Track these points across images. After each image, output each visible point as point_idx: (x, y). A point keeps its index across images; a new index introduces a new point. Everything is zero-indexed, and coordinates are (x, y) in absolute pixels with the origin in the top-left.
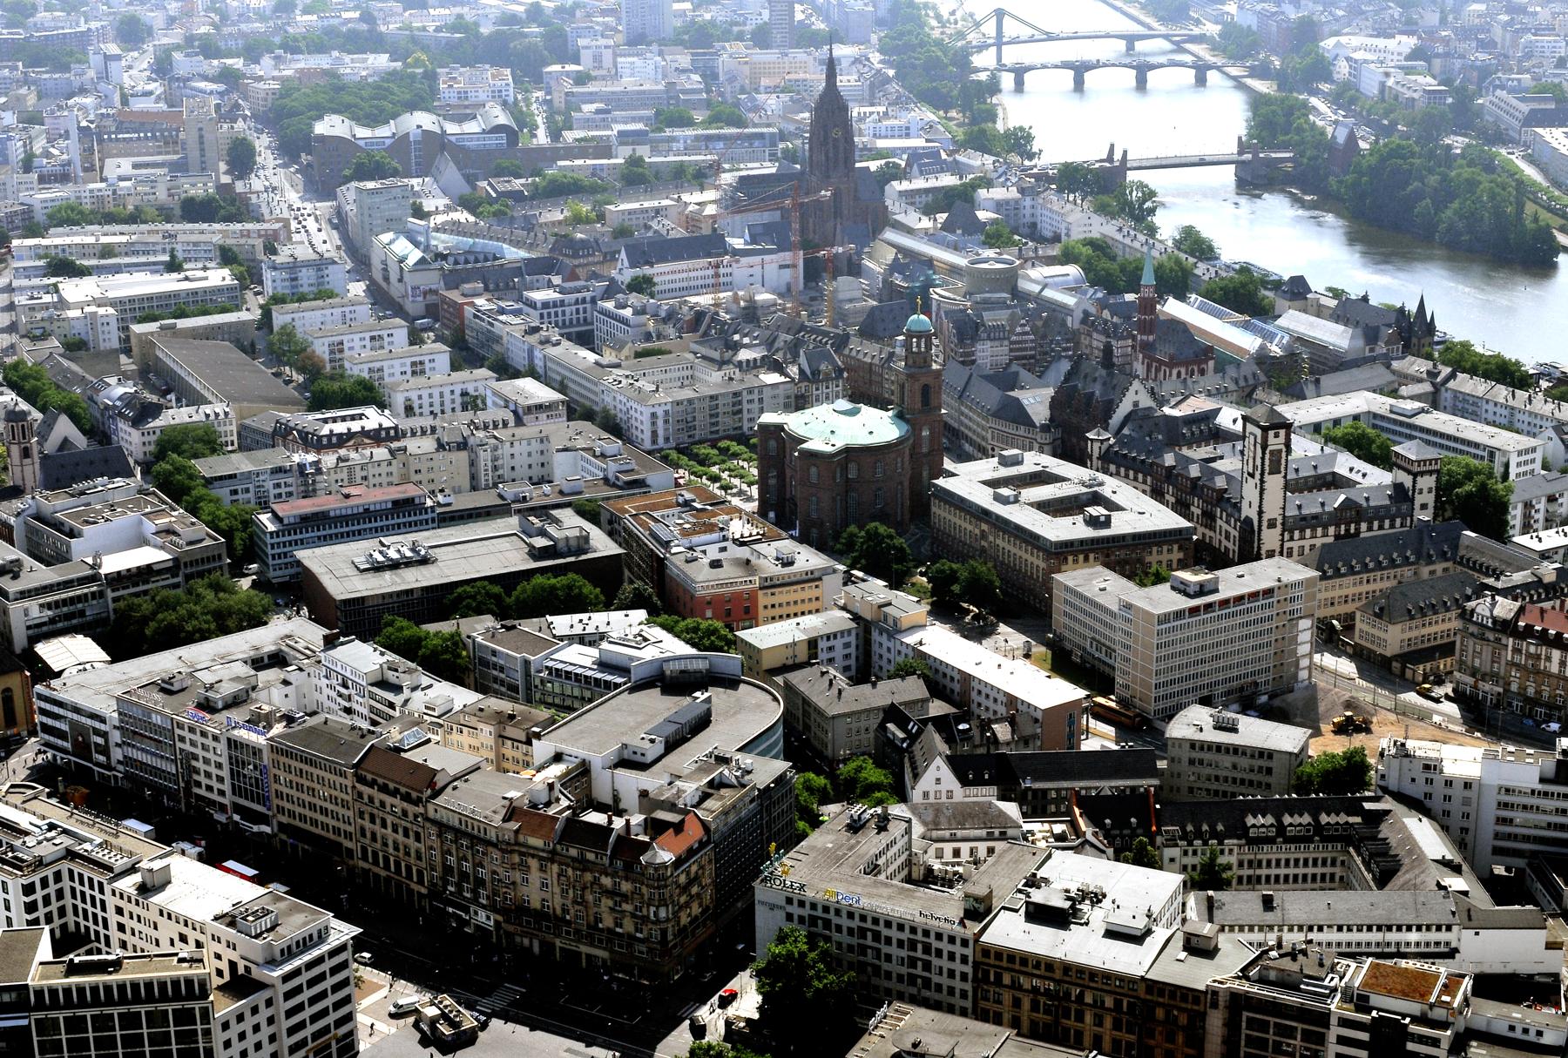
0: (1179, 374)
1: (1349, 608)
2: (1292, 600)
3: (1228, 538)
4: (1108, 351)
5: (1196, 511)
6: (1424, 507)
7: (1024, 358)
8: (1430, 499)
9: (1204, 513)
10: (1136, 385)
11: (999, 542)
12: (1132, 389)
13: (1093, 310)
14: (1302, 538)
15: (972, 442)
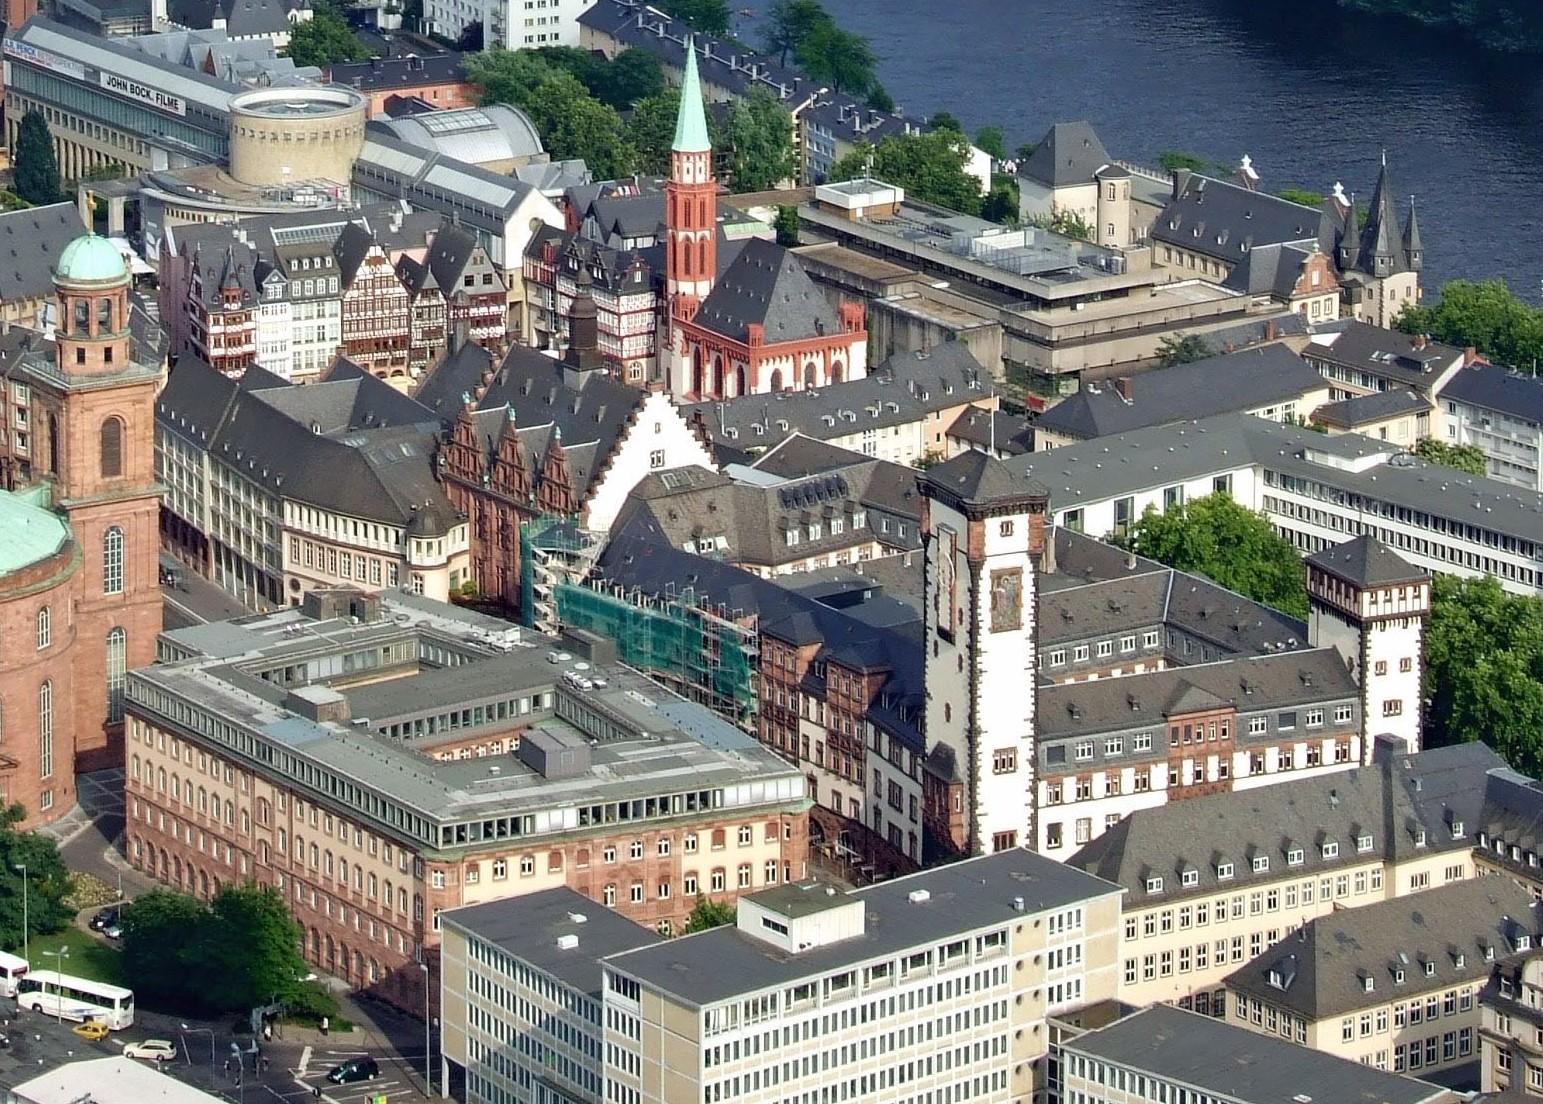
0: (776, 377)
1: (1210, 976)
2: (1055, 960)
3: (895, 802)
4: (583, 328)
5: (813, 732)
6: (1392, 707)
7: (381, 344)
8: (1407, 688)
9: (833, 736)
10: (657, 407)
11: (298, 828)
12: (645, 419)
13: (557, 220)
14: (1084, 793)
15: (242, 566)
